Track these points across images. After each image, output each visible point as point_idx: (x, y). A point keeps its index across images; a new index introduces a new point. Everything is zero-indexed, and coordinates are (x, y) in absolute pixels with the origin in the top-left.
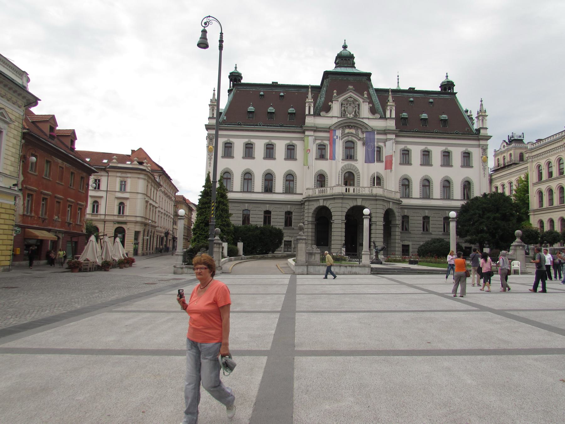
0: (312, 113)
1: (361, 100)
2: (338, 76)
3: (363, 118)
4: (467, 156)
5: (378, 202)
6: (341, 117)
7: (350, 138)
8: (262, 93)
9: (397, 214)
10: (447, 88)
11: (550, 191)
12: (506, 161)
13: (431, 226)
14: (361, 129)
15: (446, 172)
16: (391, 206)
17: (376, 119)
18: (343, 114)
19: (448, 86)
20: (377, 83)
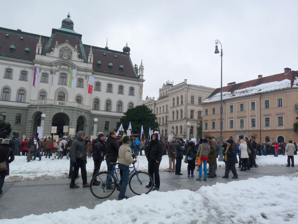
0: (40, 53)
1: (73, 50)
2: (61, 33)
3: (73, 61)
4: (132, 89)
5: (74, 112)
6: (60, 58)
7: (64, 72)
8: (7, 35)
9: (87, 119)
10: (126, 51)
11: (177, 112)
12: (164, 95)
13: (109, 127)
14: (72, 67)
15: (109, 96)
16: (83, 114)
17: (81, 62)
18: (61, 56)
19: (127, 50)
20: (85, 41)
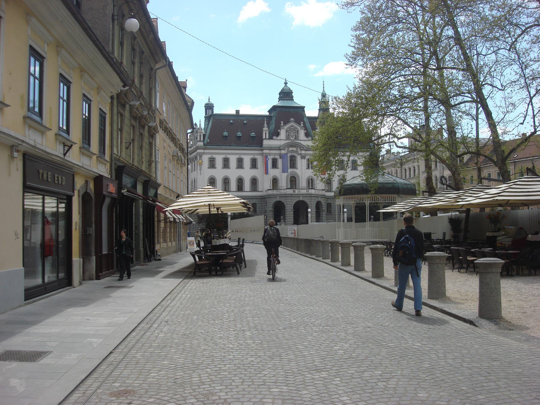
0: (267, 137)
1: (299, 128)
5: (312, 198)
6: (287, 140)
9: (323, 204)
16: (320, 199)
18: (288, 138)
